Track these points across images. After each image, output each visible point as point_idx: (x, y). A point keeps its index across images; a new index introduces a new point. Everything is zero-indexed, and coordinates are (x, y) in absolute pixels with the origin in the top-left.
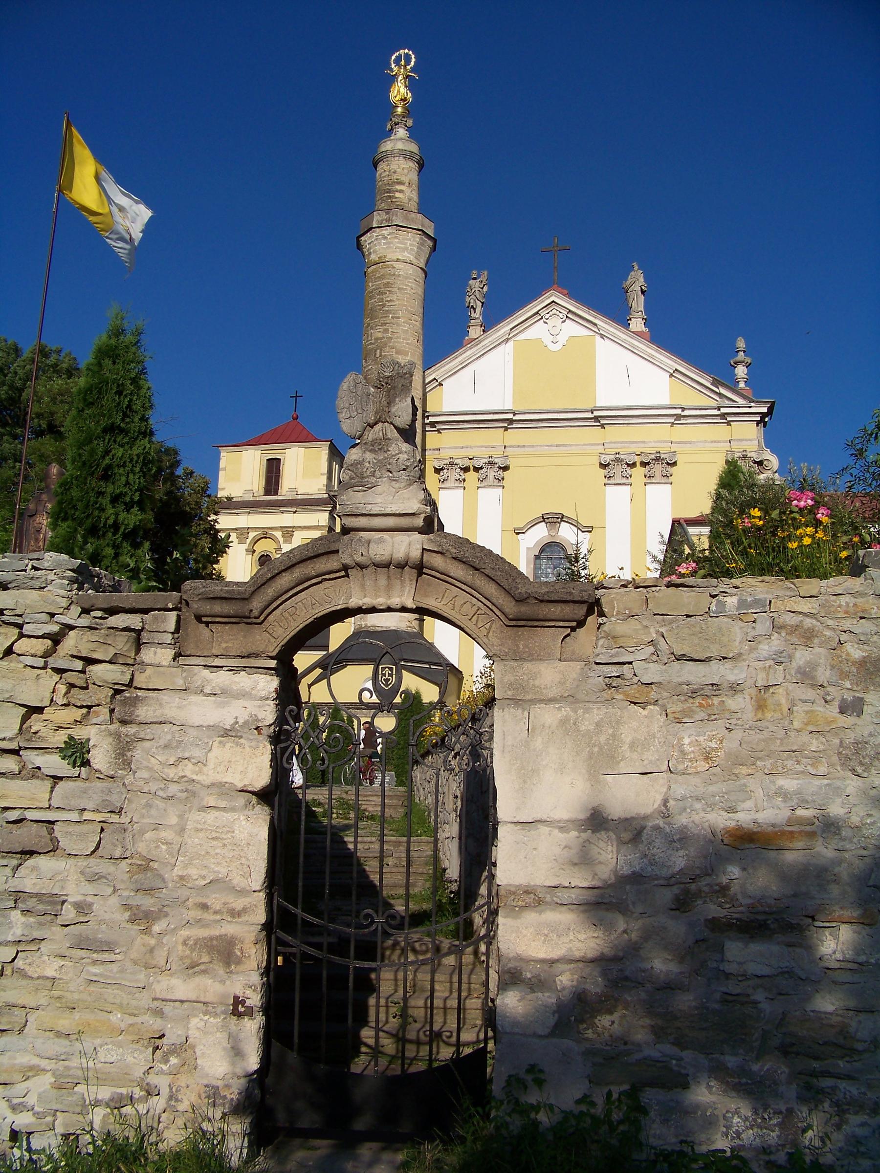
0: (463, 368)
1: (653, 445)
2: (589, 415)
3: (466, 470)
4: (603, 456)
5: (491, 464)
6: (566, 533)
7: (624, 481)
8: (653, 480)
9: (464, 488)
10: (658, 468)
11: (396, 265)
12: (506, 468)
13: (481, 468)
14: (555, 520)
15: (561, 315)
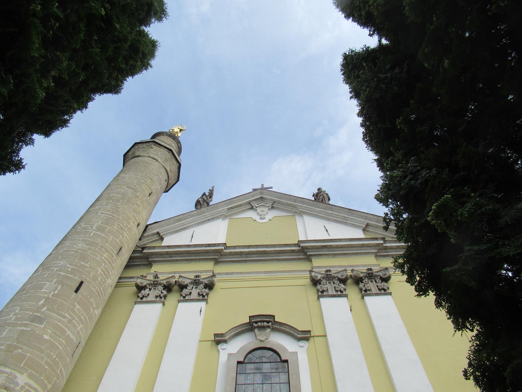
0: (184, 229)
1: (362, 268)
2: (296, 248)
3: (168, 288)
4: (313, 274)
5: (196, 282)
6: (278, 340)
7: (339, 293)
8: (368, 292)
9: (164, 304)
10: (372, 286)
11: (148, 158)
12: (210, 286)
13: (186, 287)
14: (265, 324)
15: (268, 205)
